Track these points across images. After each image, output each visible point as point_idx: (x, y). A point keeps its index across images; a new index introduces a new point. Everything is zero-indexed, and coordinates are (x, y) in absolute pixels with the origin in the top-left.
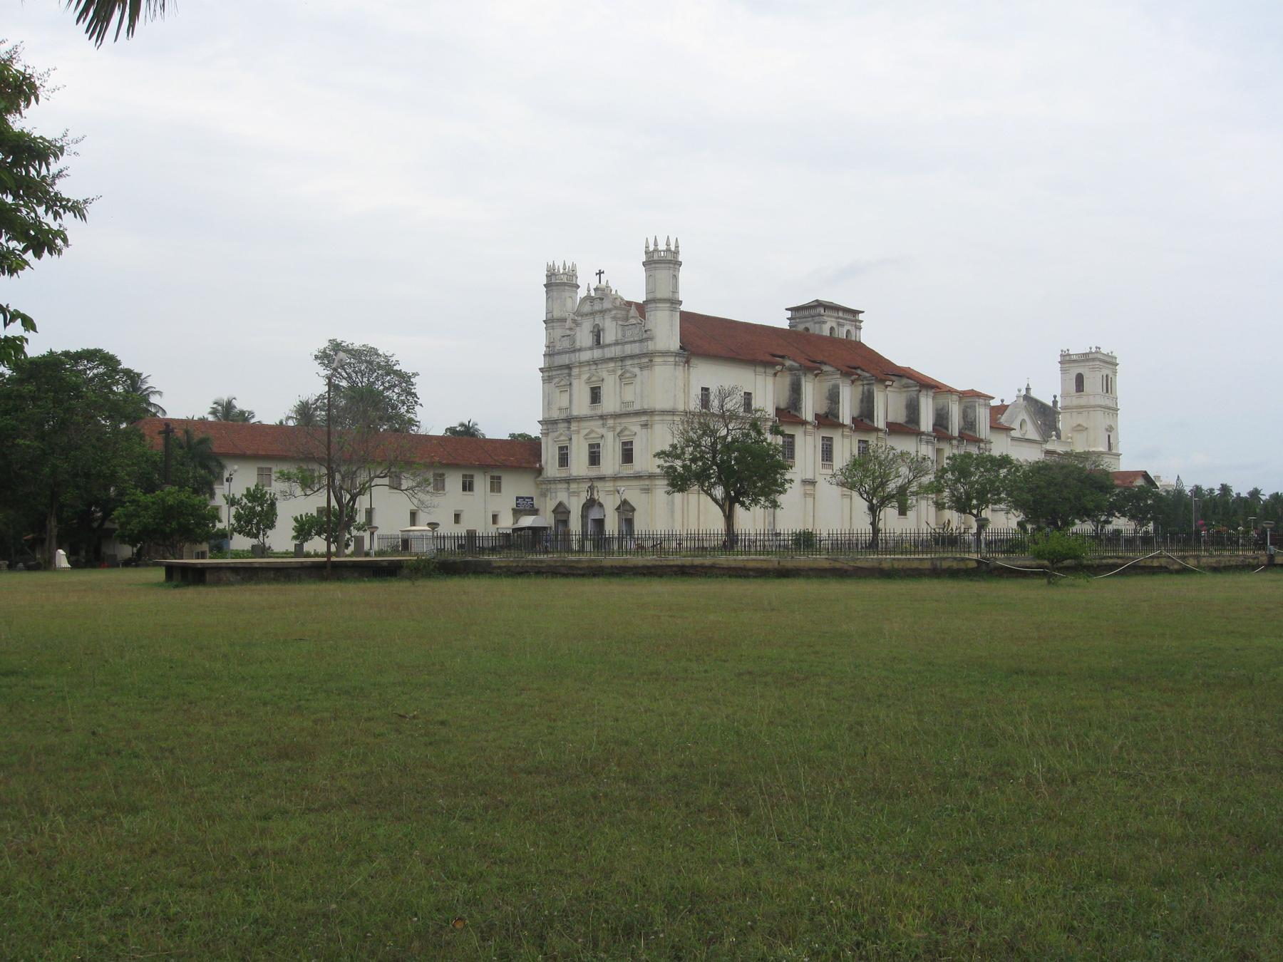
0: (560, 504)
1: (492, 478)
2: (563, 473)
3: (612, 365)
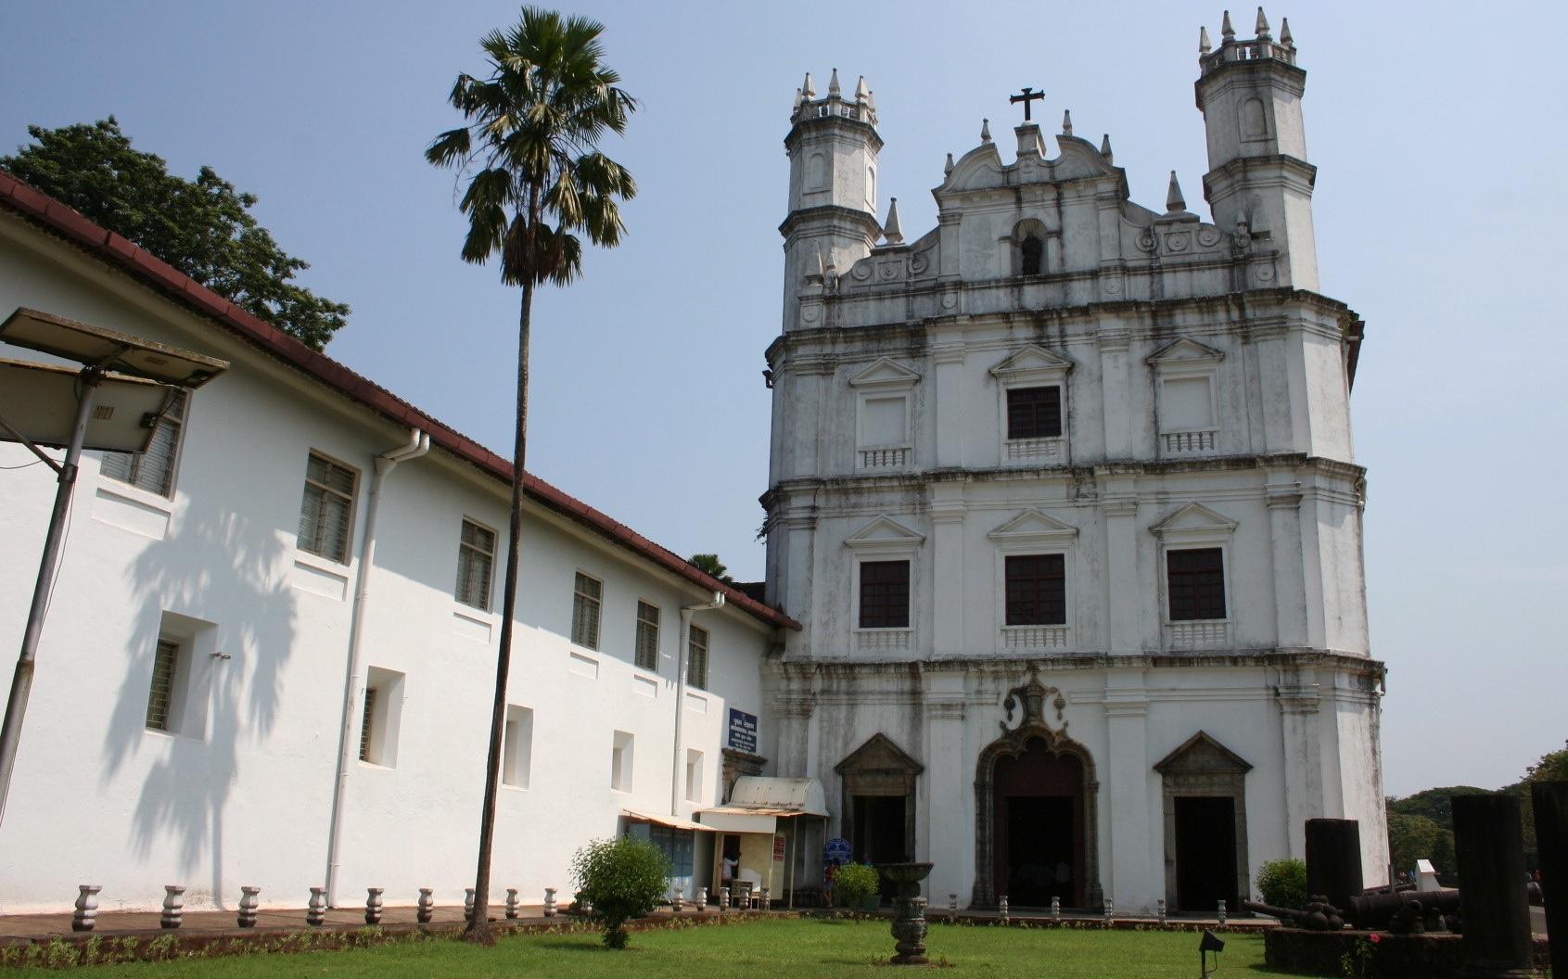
0: (879, 741)
1: (692, 627)
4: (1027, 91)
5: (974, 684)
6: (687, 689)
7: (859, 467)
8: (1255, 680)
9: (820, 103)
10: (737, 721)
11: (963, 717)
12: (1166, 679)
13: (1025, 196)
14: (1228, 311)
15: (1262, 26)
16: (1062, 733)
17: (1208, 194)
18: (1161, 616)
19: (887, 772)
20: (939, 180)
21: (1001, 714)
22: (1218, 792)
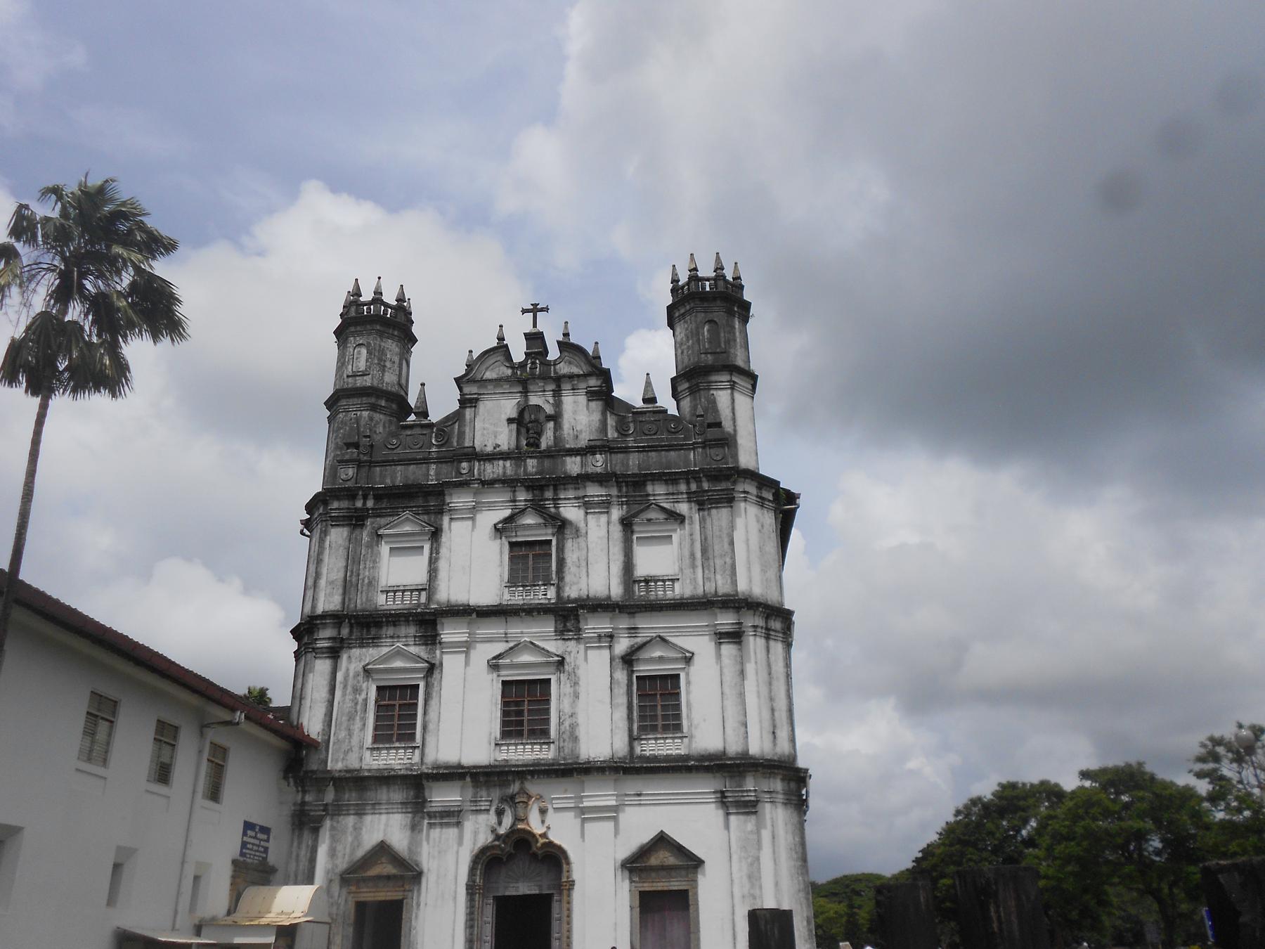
0: (383, 849)
2: (395, 759)
3: (594, 491)
4: (535, 305)
5: (469, 793)
6: (200, 801)
7: (382, 601)
8: (706, 786)
9: (369, 304)
10: (249, 832)
11: (458, 824)
12: (632, 785)
13: (531, 388)
14: (688, 483)
15: (719, 268)
16: (544, 835)
17: (675, 395)
18: (630, 730)
19: (389, 878)
20: (461, 371)
21: (492, 819)
22: (675, 885)
